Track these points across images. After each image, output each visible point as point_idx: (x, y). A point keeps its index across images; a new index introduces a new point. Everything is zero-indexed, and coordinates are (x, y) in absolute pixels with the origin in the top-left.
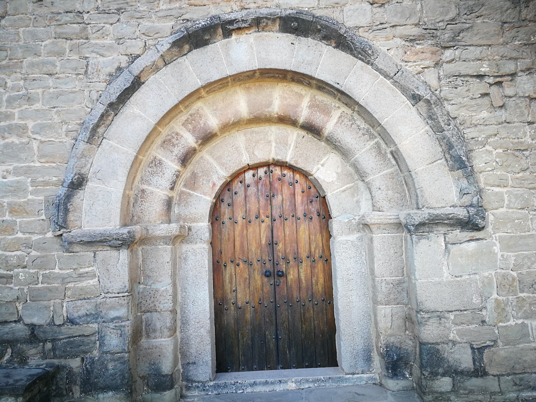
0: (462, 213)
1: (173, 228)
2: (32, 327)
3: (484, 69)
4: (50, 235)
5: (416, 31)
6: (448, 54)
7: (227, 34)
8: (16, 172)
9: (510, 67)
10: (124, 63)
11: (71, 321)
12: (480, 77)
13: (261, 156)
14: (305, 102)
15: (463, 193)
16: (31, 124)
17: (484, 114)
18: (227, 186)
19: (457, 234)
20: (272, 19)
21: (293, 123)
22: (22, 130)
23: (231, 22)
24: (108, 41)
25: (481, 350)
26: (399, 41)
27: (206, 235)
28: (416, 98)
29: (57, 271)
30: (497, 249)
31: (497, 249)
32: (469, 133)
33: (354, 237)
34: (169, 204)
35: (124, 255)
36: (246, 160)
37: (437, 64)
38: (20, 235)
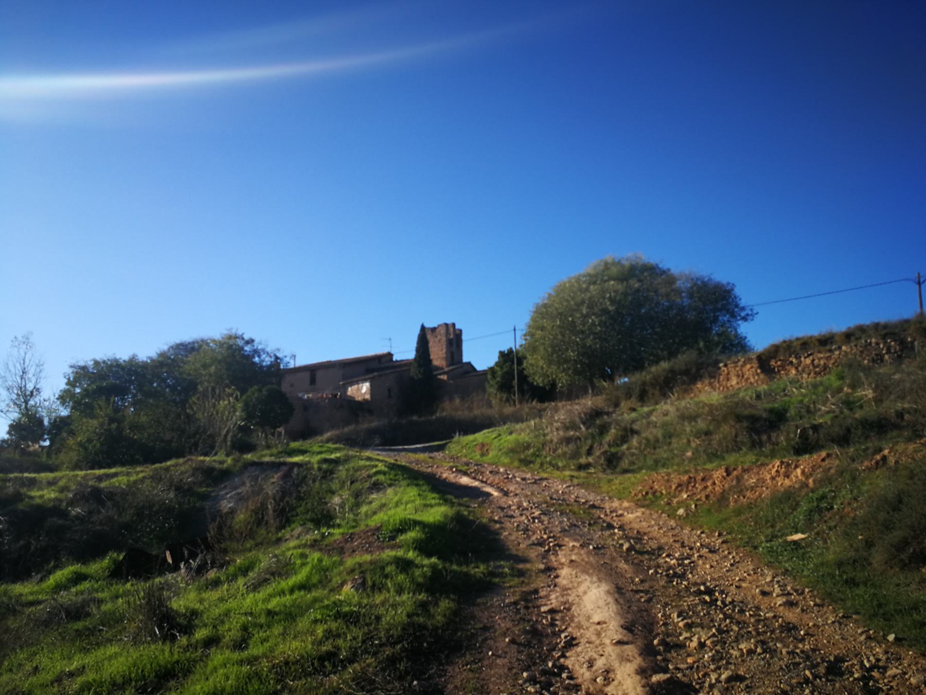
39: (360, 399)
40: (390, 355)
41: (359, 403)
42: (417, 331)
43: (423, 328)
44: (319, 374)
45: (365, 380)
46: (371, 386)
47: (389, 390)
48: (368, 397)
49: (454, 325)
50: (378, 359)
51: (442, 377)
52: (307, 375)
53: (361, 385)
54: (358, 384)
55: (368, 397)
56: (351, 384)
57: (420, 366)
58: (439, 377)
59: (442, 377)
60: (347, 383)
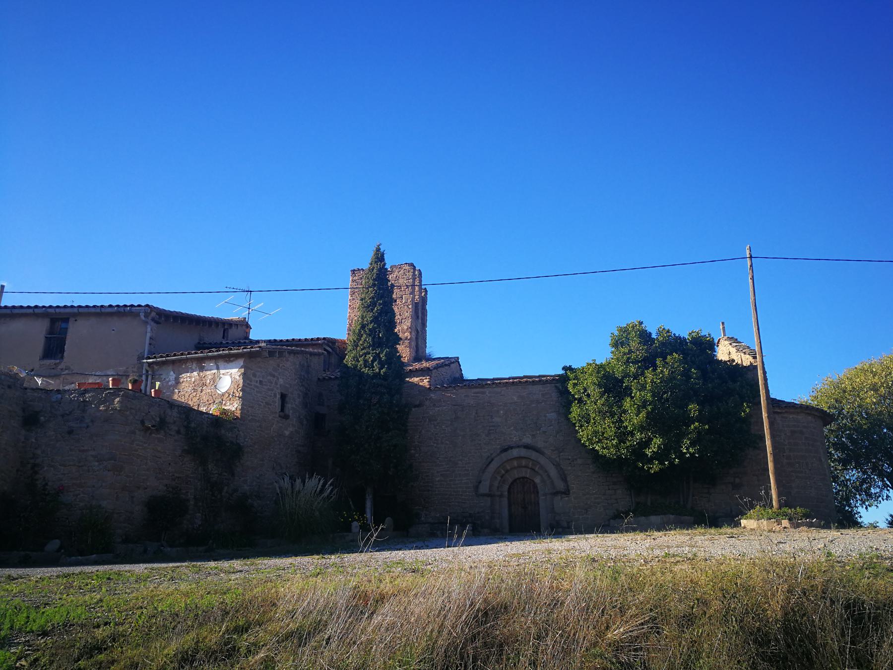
0: (563, 490)
1: (499, 493)
2: (470, 514)
3: (570, 458)
4: (474, 494)
5: (554, 449)
6: (562, 454)
7: (512, 449)
8: (467, 479)
9: (575, 457)
10: (489, 454)
11: (478, 513)
12: (569, 459)
13: (521, 475)
14: (530, 463)
15: (564, 486)
16: (470, 469)
17: (570, 468)
18: (512, 483)
19: (563, 496)
20: (522, 446)
21: (528, 468)
22: (468, 470)
23: (512, 447)
24: (486, 450)
25: (569, 522)
26: (550, 451)
27: (507, 496)
28: (554, 464)
29: (475, 501)
30: (573, 499)
31: (573, 499)
32: (566, 472)
33: (544, 497)
34: (498, 488)
35: (489, 499)
36: (517, 476)
37: (559, 456)
38: (467, 493)
39: (213, 410)
40: (244, 325)
41: (218, 422)
42: (365, 262)
43: (379, 257)
44: (76, 331)
45: (229, 359)
46: (245, 376)
47: (283, 397)
48: (234, 406)
49: (420, 274)
50: (225, 326)
51: (415, 380)
52: (39, 329)
53: (209, 374)
54: (202, 369)
55: (234, 406)
56: (181, 365)
57: (377, 343)
58: (407, 379)
59: (415, 380)
60: (163, 363)
